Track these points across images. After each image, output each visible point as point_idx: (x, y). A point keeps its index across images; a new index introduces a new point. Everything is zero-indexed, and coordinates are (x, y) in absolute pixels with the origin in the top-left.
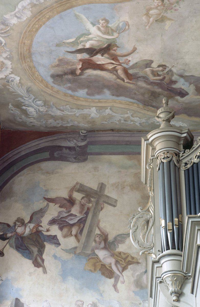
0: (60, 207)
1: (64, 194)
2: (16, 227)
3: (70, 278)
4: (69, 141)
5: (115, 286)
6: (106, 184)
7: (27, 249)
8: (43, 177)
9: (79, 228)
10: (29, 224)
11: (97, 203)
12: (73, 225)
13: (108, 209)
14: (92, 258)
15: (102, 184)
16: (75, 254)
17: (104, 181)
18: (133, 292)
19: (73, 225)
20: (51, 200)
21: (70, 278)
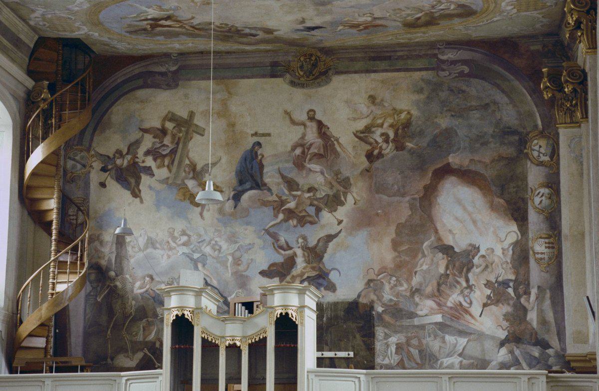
0: (154, 137)
1: (158, 125)
2: (116, 159)
3: (162, 207)
4: (162, 65)
5: (201, 214)
6: (195, 111)
7: (126, 180)
8: (138, 106)
9: (171, 158)
10: (127, 156)
11: (187, 133)
12: (165, 156)
13: (197, 138)
14: (183, 188)
15: (192, 112)
16: (167, 184)
17: (194, 109)
18: (217, 219)
19: (165, 156)
20: (146, 131)
21: (162, 207)
